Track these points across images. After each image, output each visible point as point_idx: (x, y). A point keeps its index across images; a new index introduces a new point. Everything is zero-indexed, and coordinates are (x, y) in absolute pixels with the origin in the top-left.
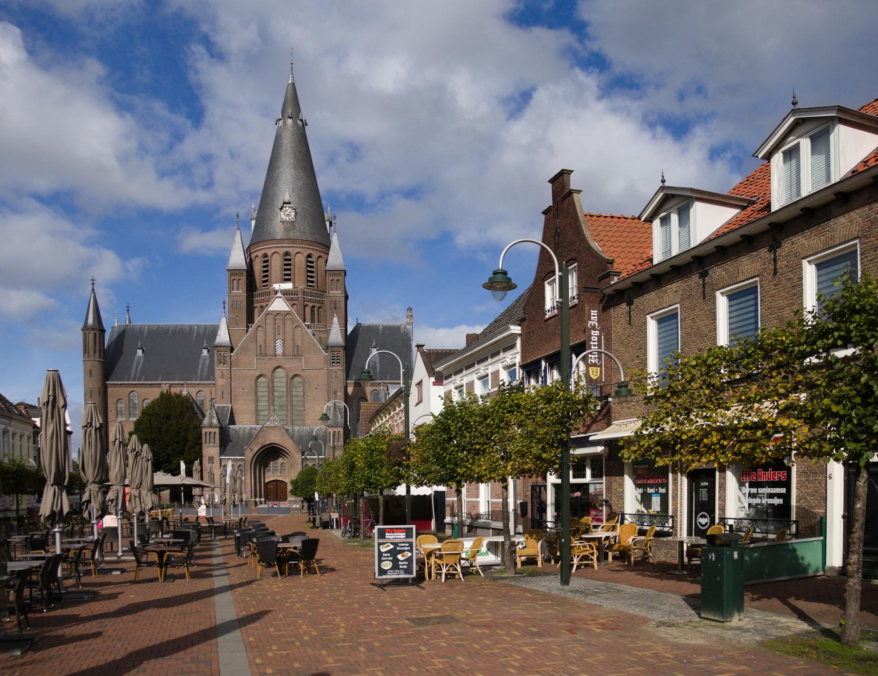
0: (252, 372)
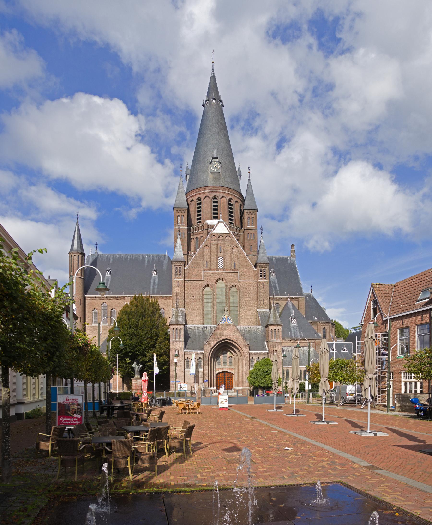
0: (200, 283)
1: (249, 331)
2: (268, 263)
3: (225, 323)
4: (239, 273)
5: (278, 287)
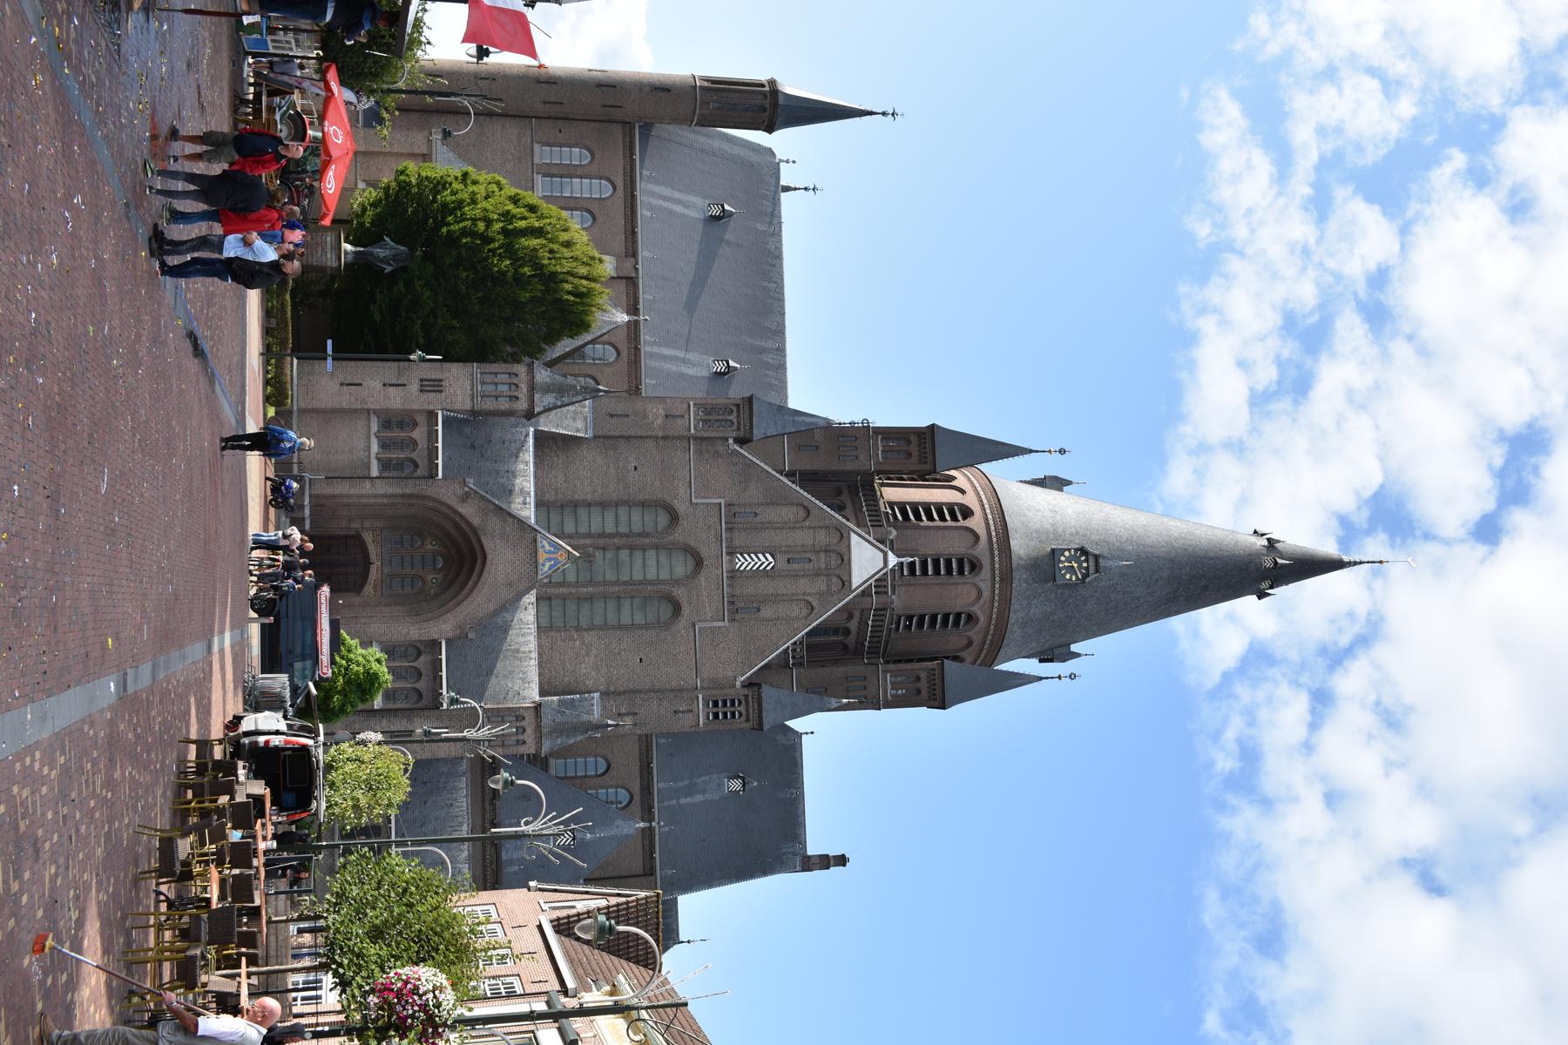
0: (682, 491)
1: (517, 651)
2: (761, 728)
3: (540, 551)
4: (721, 624)
5: (689, 800)
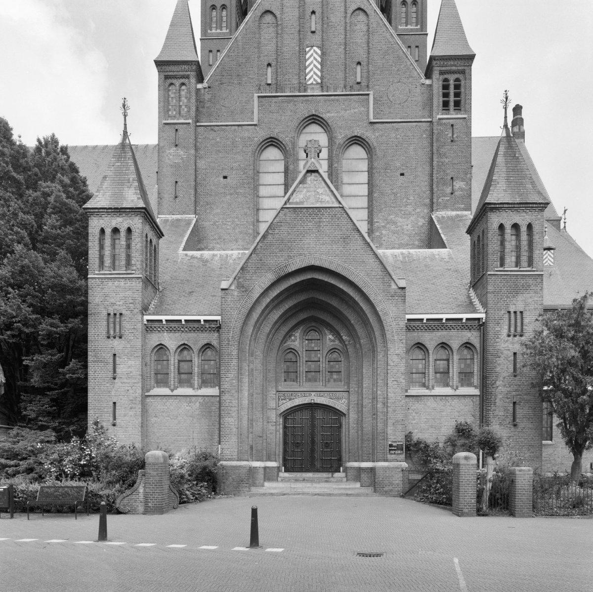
0: (246, 133)
4: (371, 98)
